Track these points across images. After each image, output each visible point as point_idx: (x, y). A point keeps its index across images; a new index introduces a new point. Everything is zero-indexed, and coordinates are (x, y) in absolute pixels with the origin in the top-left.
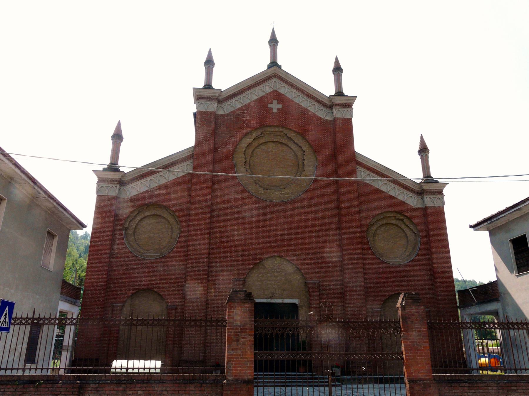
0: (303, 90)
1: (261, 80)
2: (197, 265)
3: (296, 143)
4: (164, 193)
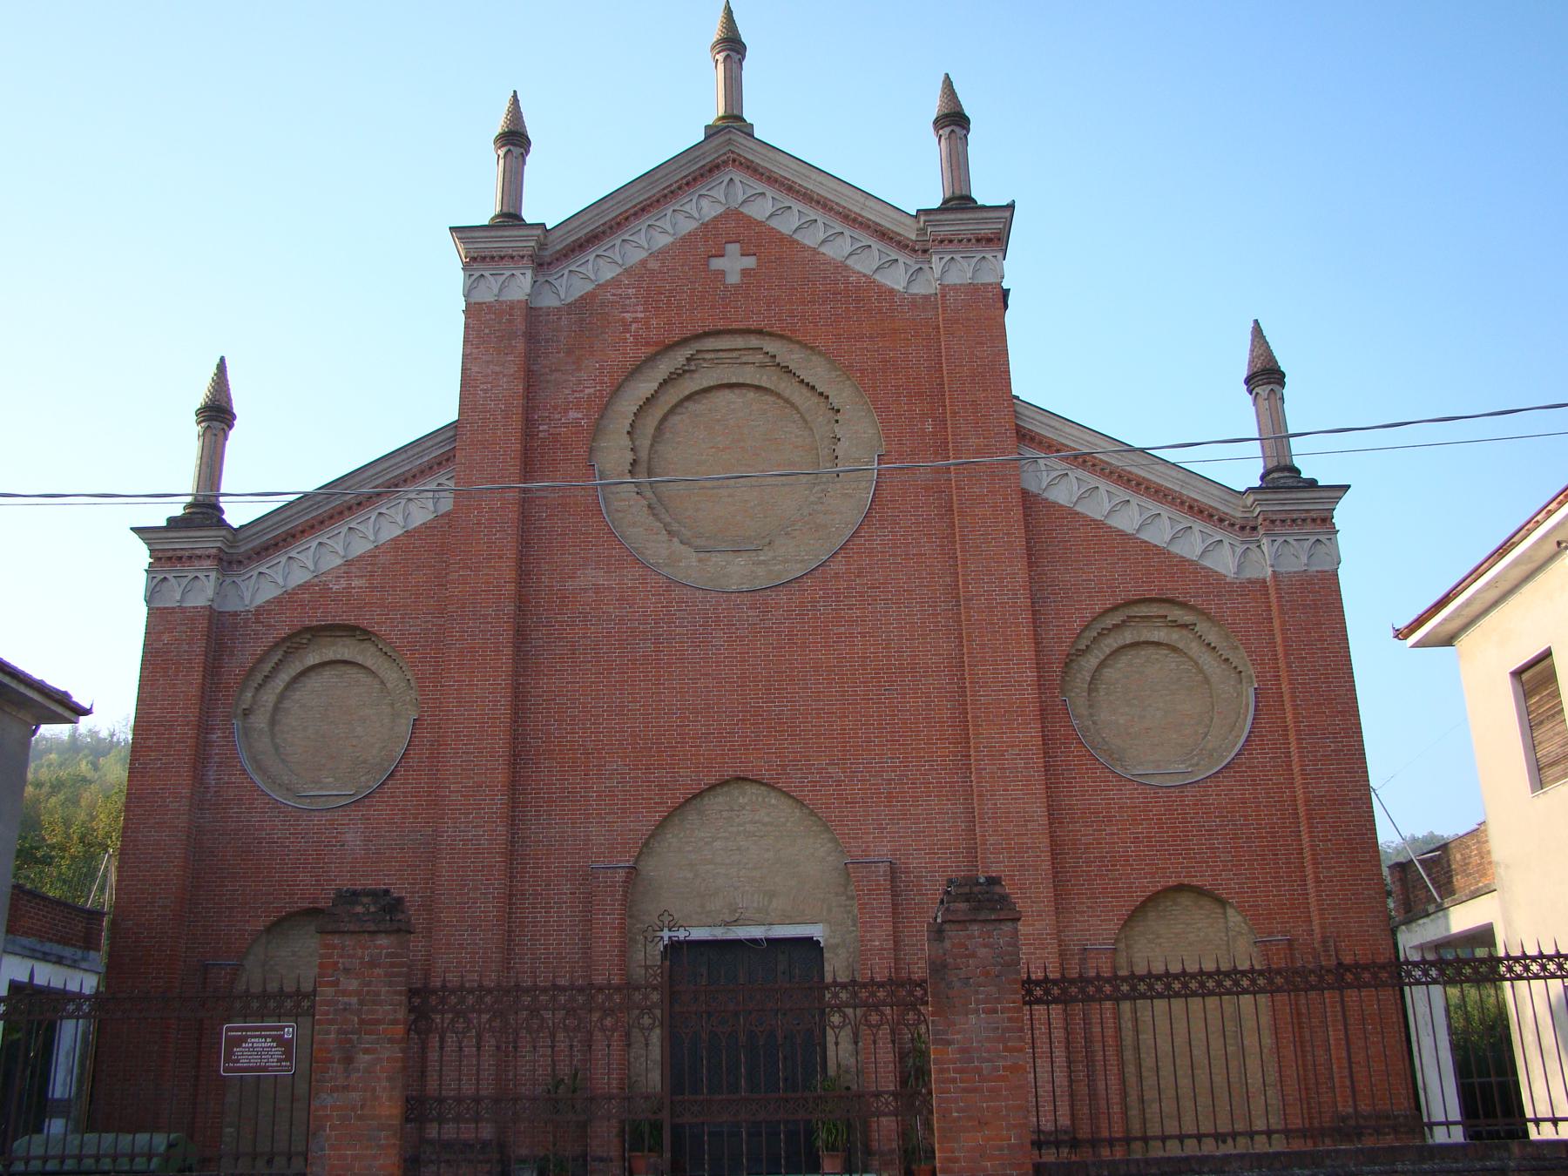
0: (830, 200)
1: (684, 181)
2: (472, 822)
3: (808, 384)
4: (361, 588)
